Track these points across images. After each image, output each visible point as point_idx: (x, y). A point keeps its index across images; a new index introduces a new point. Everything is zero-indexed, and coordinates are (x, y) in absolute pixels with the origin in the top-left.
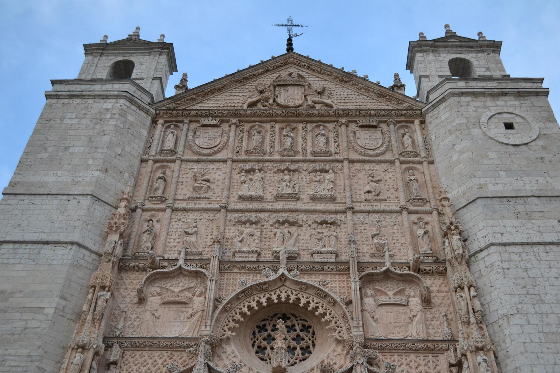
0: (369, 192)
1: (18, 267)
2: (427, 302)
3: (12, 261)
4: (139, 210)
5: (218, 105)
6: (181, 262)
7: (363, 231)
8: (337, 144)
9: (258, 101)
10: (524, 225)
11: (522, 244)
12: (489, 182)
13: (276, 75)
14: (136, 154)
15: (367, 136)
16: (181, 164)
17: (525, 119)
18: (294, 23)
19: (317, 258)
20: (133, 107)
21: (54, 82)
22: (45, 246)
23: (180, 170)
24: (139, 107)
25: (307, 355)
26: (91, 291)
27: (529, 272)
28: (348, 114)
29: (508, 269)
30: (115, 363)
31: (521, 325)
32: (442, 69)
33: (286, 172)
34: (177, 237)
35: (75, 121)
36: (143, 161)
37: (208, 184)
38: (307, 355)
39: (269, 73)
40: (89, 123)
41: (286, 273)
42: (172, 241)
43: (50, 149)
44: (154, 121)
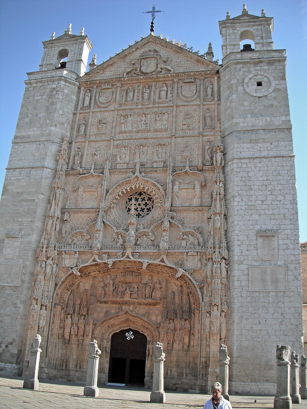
0: (184, 125)
1: (23, 180)
2: (203, 186)
3: (20, 178)
4: (73, 143)
5: (111, 75)
6: (92, 171)
7: (179, 148)
8: (171, 95)
9: (132, 70)
10: (253, 147)
11: (249, 158)
12: (241, 121)
13: (143, 51)
14: (70, 111)
15: (188, 89)
16: (93, 114)
17: (269, 79)
18: (156, 10)
19: (155, 165)
20: (67, 84)
21: (28, 74)
22: (32, 169)
23: (92, 118)
24: (70, 83)
25: (149, 212)
26: (53, 190)
27: (249, 174)
29: (239, 172)
30: (66, 220)
31: (238, 202)
32: (235, 39)
33: (144, 115)
34: (91, 156)
35: (39, 98)
38: (149, 212)
39: (139, 50)
40: (46, 98)
42: (88, 158)
43: (30, 116)
44: (79, 88)
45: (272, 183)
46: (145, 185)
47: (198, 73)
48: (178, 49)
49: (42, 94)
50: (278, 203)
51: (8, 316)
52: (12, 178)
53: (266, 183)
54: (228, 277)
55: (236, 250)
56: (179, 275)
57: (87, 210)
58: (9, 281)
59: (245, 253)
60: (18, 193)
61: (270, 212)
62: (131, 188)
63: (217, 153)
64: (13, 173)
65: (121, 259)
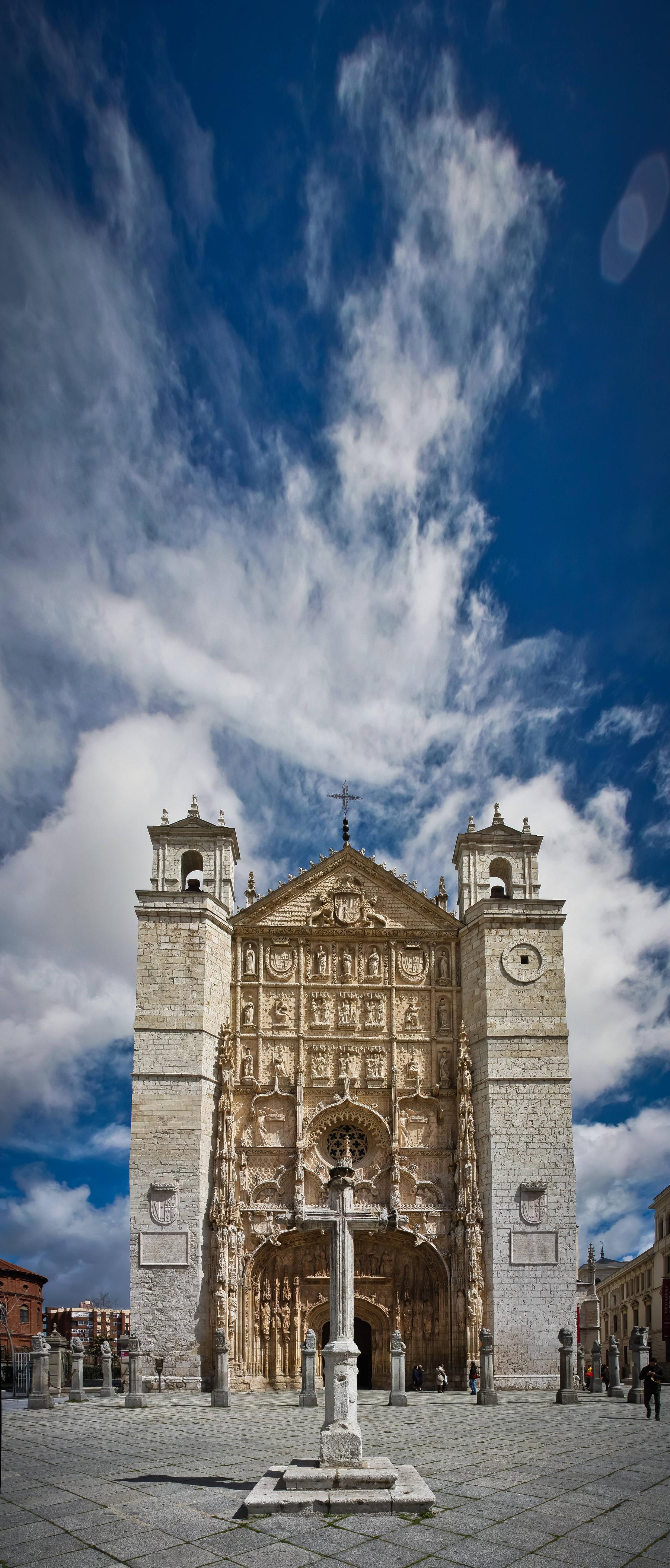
6: (277, 1088)
9: (321, 915)
36: (233, 987)
37: (287, 1012)
45: (540, 1118)
48: (395, 883)
50: (548, 1146)
51: (177, 1309)
53: (532, 1117)
54: (483, 1245)
55: (495, 1209)
56: (419, 1242)
58: (171, 1258)
59: (506, 1213)
61: (538, 1159)
63: (464, 1070)
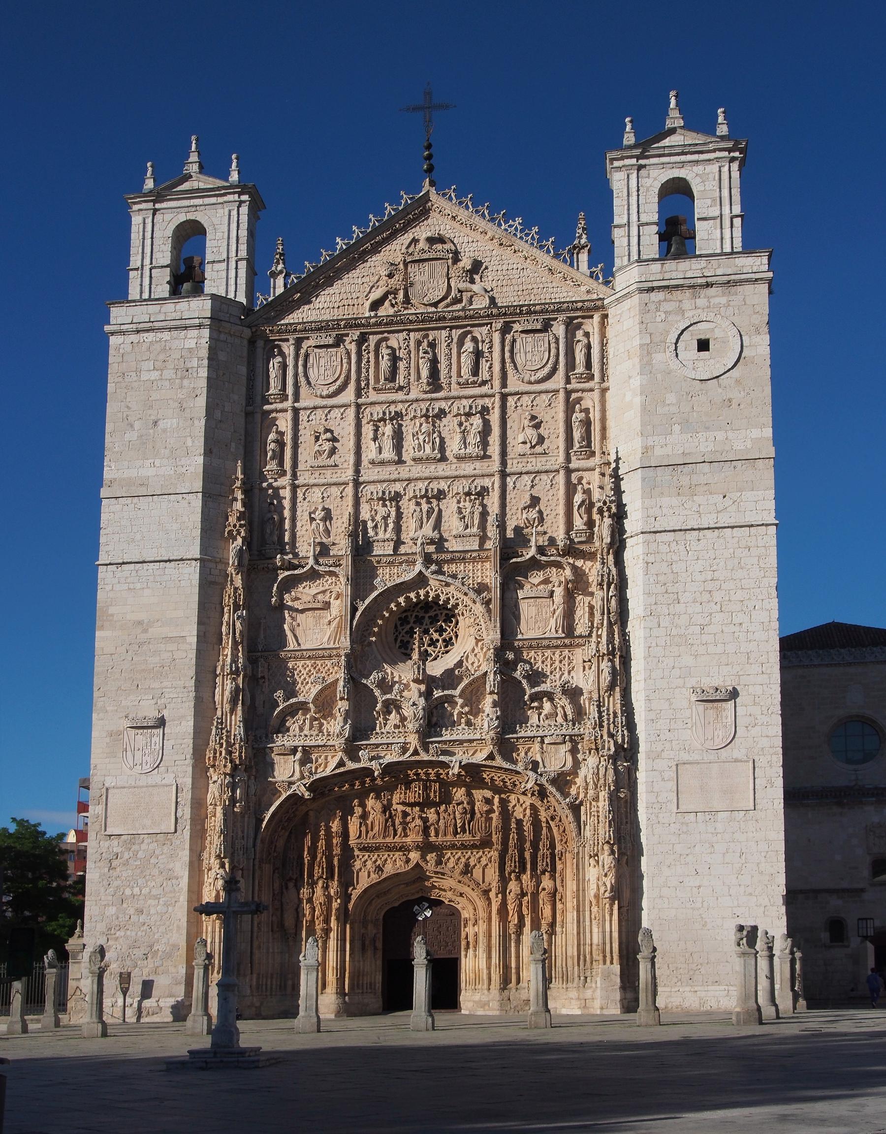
0: (524, 443)
1: (147, 592)
3: (138, 586)
6: (311, 562)
15: (529, 349)
28: (505, 314)
41: (424, 570)
43: (137, 425)
46: (439, 591)
47: (552, 307)
49: (159, 364)
52: (117, 587)
57: (310, 653)
60: (140, 623)
62: (408, 599)
64: (118, 575)
65: (401, 759)
